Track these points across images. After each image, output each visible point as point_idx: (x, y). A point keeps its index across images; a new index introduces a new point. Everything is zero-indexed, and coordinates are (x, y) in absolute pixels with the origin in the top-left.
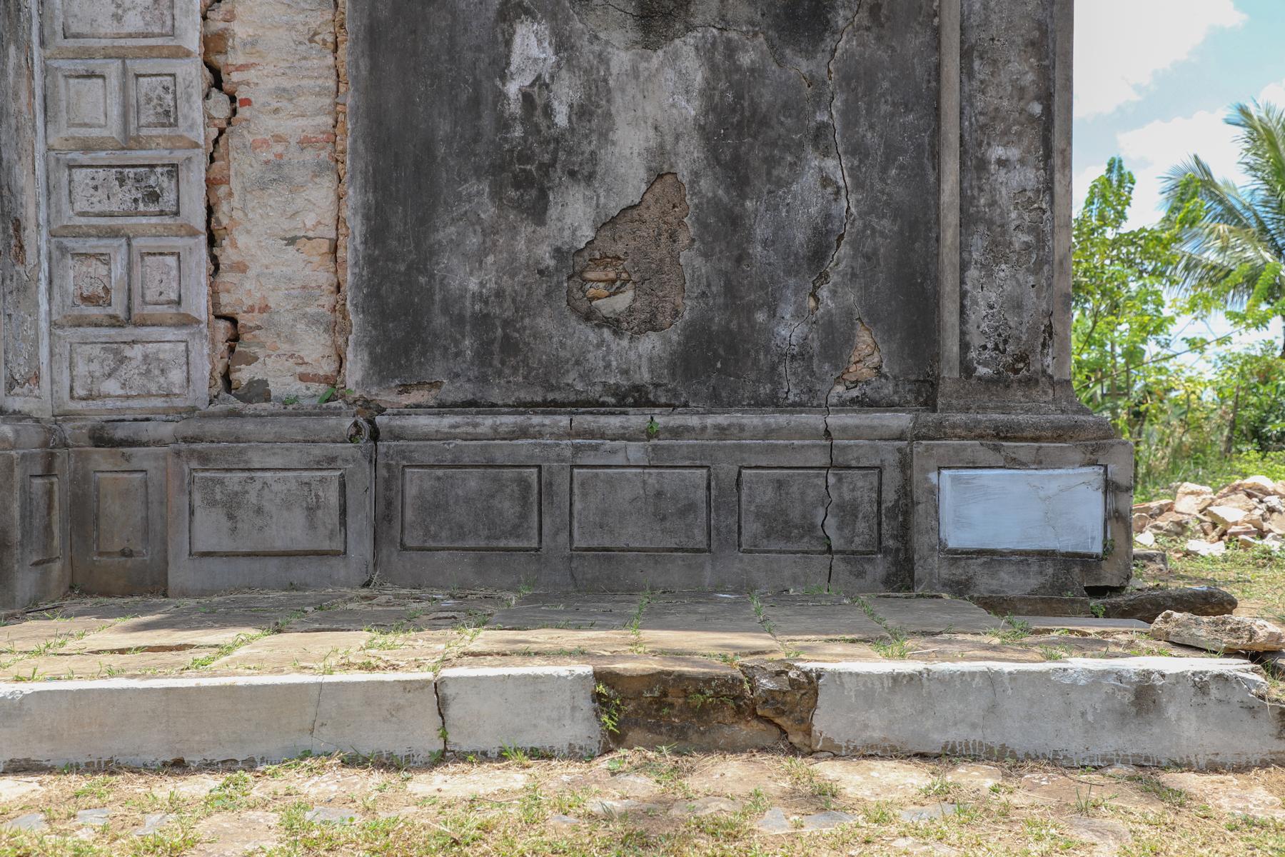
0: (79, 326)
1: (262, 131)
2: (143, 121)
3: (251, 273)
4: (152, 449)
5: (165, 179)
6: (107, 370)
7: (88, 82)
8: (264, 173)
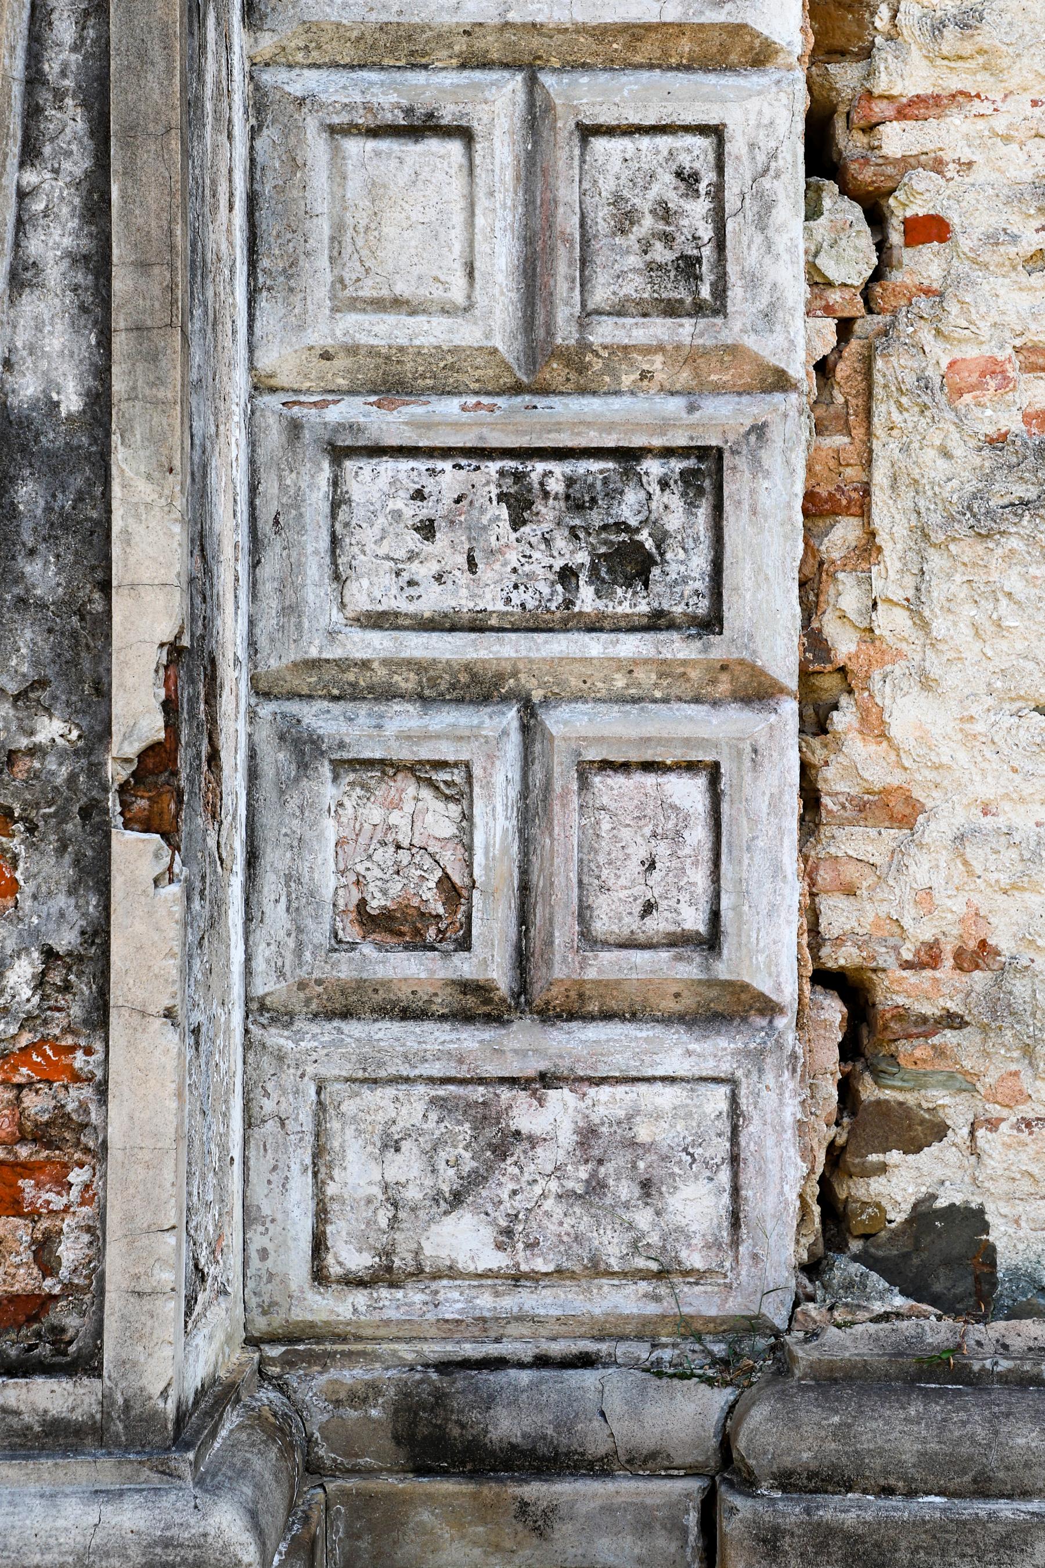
0: (346, 1015)
1: (985, 330)
2: (601, 295)
5: (675, 501)
6: (448, 1179)
7: (414, 151)
8: (989, 478)
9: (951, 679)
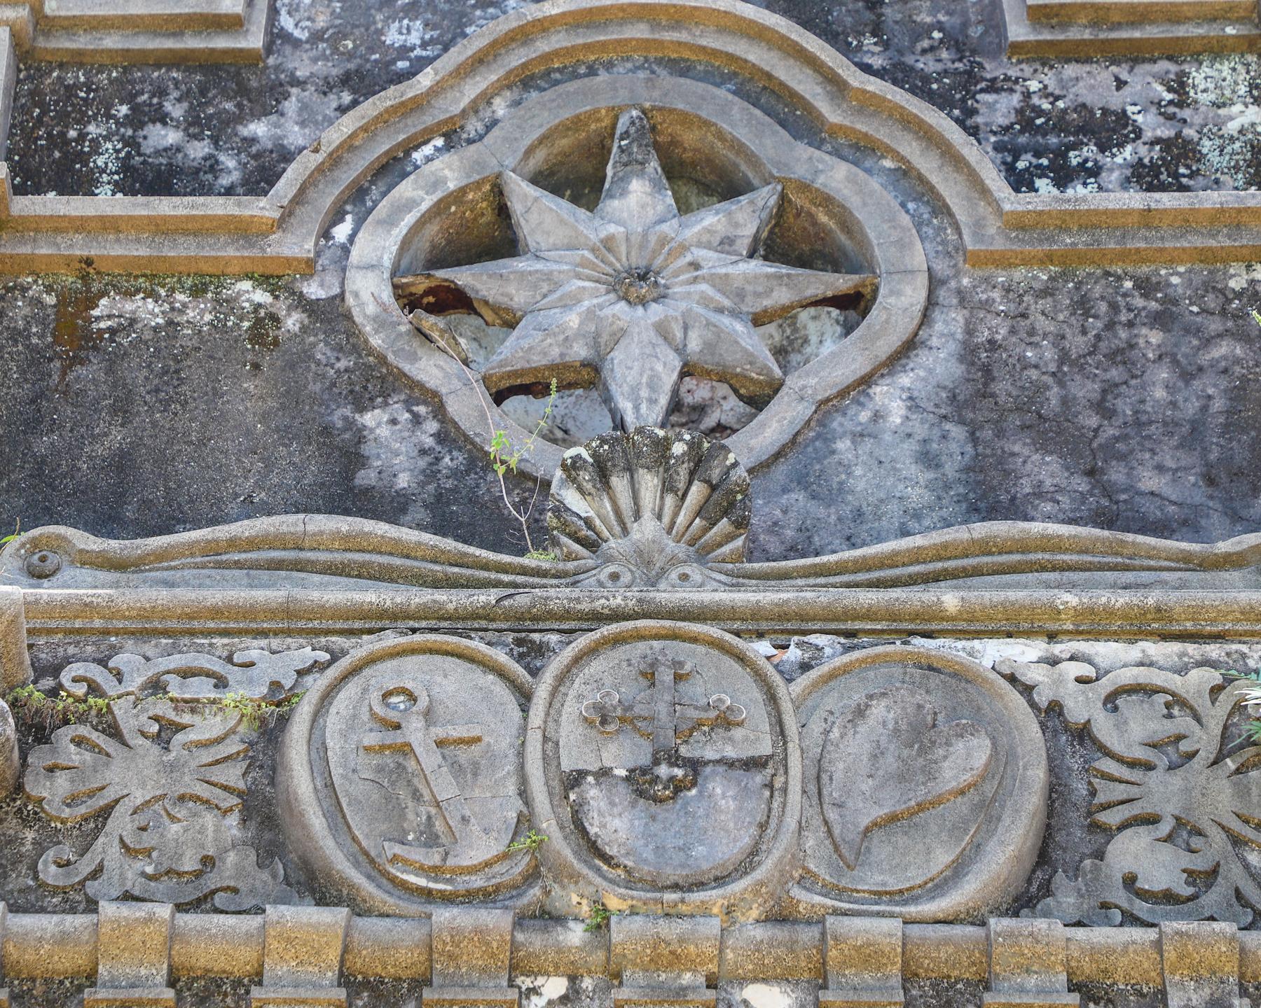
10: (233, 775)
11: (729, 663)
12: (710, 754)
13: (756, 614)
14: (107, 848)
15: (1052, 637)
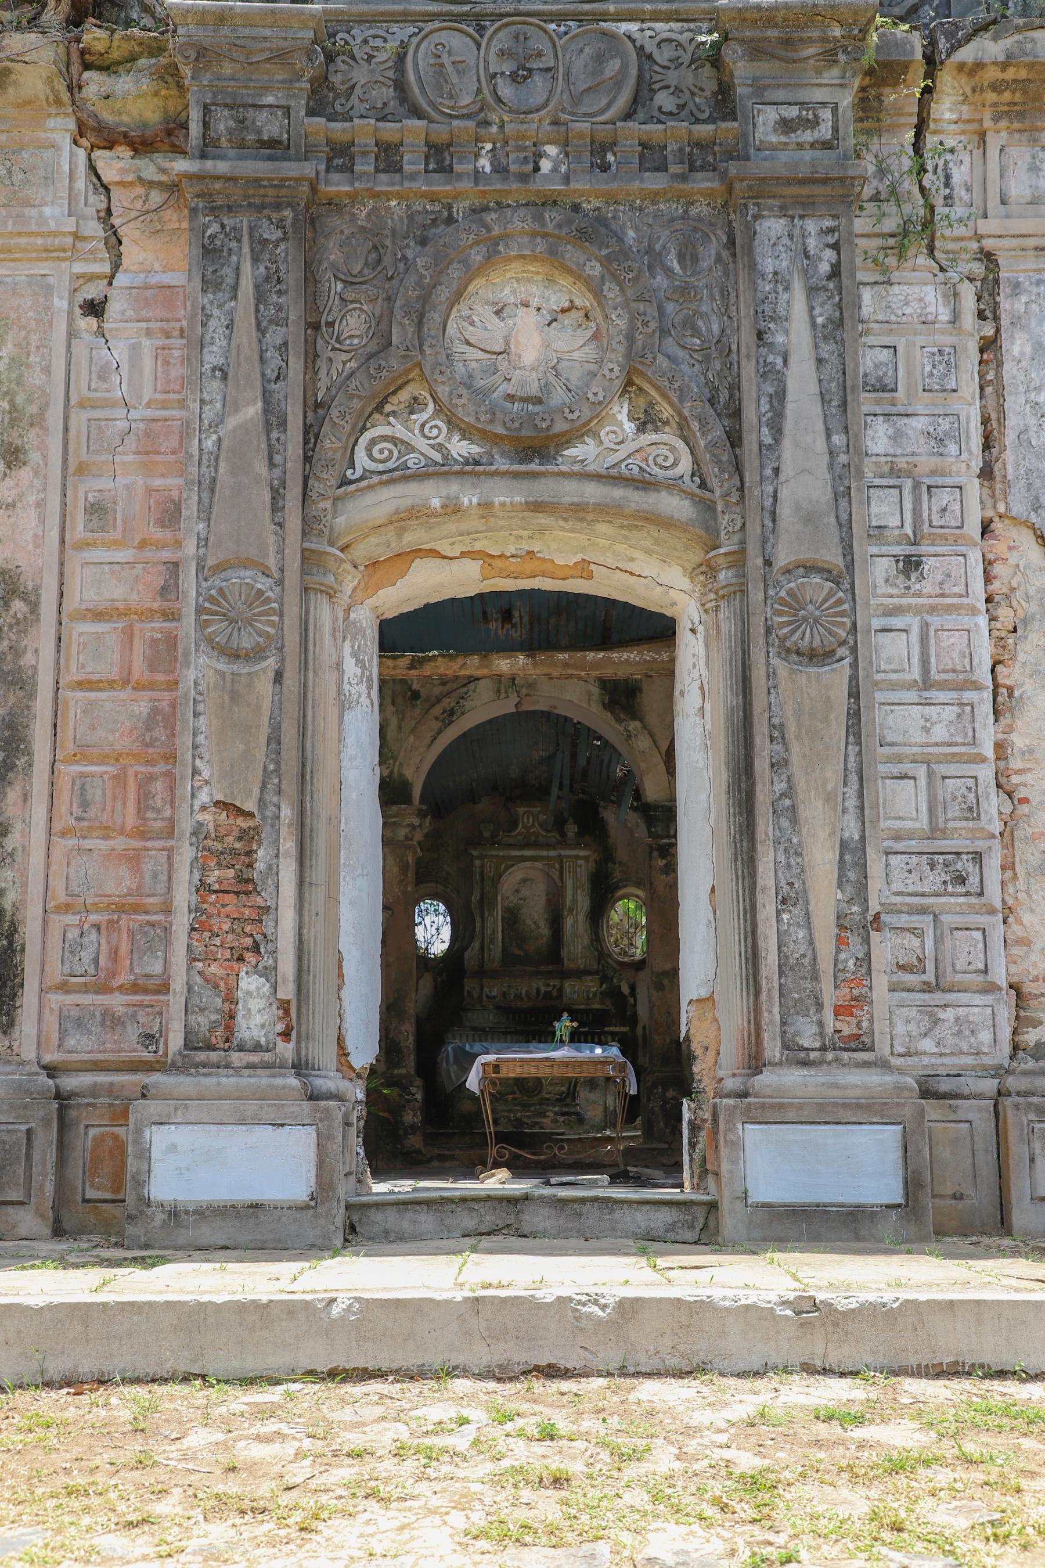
2: (949, 816)
3: (1037, 946)
4: (972, 1102)
5: (970, 864)
6: (923, 1030)
9: (1038, 910)
10: (390, 74)
11: (541, 33)
12: (535, 66)
13: (551, 13)
14: (354, 99)
15: (643, 21)
